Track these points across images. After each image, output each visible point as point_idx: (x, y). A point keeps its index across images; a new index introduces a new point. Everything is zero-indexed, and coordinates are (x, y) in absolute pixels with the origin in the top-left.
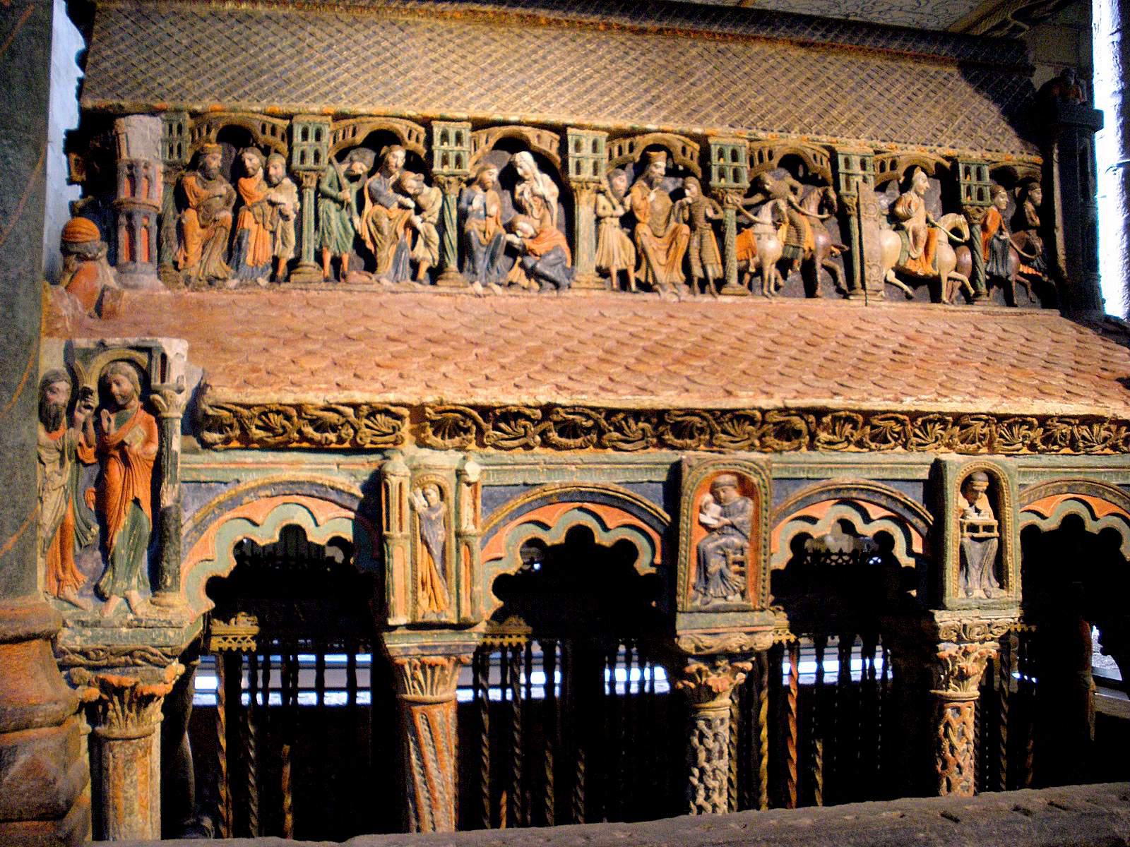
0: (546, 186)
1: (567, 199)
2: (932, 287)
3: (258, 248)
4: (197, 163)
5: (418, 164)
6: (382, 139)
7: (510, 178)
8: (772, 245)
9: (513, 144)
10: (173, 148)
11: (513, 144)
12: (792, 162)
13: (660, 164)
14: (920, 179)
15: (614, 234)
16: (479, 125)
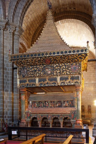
0: (47, 103)
1: (48, 104)
2: (66, 106)
3: (35, 107)
4: (33, 103)
5: (42, 103)
6: (40, 102)
7: (46, 103)
8: (58, 105)
9: (46, 101)
10: (32, 102)
11: (46, 101)
12: (59, 101)
13: (52, 102)
14: (66, 101)
15: (50, 105)
16: (44, 101)
